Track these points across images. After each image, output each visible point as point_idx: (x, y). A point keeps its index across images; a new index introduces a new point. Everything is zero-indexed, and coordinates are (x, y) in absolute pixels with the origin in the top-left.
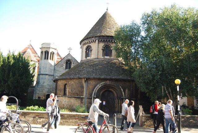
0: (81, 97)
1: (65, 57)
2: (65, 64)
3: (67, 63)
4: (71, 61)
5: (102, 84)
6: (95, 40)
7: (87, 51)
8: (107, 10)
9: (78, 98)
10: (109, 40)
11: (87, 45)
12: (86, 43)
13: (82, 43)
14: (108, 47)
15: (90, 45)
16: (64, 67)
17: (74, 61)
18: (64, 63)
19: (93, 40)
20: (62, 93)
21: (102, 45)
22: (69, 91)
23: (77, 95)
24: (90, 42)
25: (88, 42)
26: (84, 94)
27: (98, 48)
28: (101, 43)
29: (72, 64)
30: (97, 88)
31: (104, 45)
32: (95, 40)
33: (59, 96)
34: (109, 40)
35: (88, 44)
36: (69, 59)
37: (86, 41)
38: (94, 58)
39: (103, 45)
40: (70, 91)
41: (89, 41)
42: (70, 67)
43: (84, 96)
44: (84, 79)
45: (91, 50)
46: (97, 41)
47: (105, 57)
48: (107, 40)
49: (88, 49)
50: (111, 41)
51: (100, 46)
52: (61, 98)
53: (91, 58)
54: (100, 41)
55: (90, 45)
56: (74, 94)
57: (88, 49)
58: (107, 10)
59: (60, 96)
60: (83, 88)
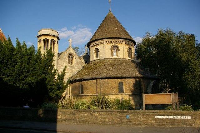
2: (68, 58)
6: (122, 41)
9: (136, 94)
13: (105, 41)
15: (117, 44)
16: (67, 61)
21: (126, 47)
22: (126, 89)
23: (136, 92)
24: (118, 42)
25: (115, 42)
26: (143, 91)
29: (74, 58)
32: (123, 42)
35: (114, 44)
37: (113, 40)
39: (128, 47)
42: (72, 64)
46: (124, 43)
53: (119, 58)
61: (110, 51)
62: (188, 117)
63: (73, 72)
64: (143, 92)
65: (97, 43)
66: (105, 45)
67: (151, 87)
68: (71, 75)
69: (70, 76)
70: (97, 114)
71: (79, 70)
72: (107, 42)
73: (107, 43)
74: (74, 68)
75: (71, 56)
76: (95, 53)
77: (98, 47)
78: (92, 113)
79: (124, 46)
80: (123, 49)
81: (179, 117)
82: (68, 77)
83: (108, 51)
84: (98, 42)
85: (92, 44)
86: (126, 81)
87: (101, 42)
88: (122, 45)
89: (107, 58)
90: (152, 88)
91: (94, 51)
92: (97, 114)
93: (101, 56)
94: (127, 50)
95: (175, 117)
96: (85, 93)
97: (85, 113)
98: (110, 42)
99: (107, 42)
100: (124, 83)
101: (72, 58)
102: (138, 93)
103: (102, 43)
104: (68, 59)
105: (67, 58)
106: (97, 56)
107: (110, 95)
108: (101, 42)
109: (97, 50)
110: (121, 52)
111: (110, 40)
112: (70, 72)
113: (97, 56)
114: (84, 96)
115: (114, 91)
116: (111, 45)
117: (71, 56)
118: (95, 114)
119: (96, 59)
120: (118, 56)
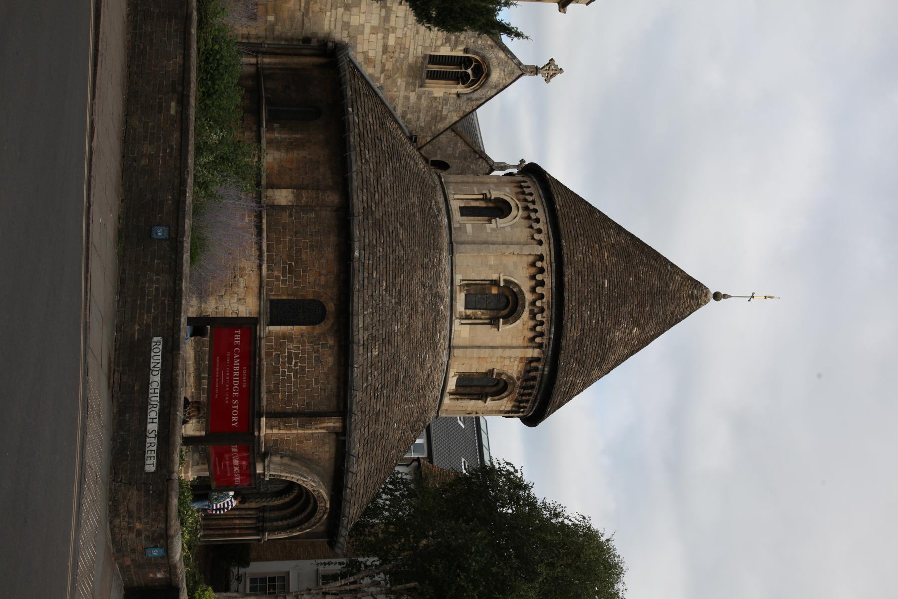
0: (263, 420)
1: (502, 55)
2: (459, 53)
3: (464, 62)
4: (474, 82)
5: (320, 492)
7: (494, 291)
8: (717, 296)
10: (530, 394)
11: (525, 285)
12: (539, 290)
13: (543, 250)
14: (502, 385)
15: (526, 314)
17: (476, 95)
18: (466, 50)
19: (541, 334)
20: (283, 290)
22: (289, 338)
23: (269, 391)
24: (539, 317)
25: (538, 303)
26: (275, 431)
27: (501, 357)
28: (521, 365)
29: (461, 89)
30: (304, 481)
31: (511, 378)
32: (540, 346)
33: (260, 267)
34: (530, 394)
35: (529, 297)
36: (488, 75)
38: (455, 342)
39: (510, 372)
40: (291, 346)
41: (542, 310)
42: (434, 76)
43: (269, 432)
44: (344, 427)
45: (494, 322)
46: (535, 353)
47: (455, 379)
48: (532, 387)
49: (507, 293)
50: (524, 398)
51: (507, 362)
52: (255, 284)
53: (456, 322)
54: (533, 364)
55: (526, 314)
56: (275, 371)
57: (507, 293)
58: (717, 296)
59: (264, 267)
60: (302, 426)
61: (495, 277)
62: (153, 461)
63: (389, 82)
64: (272, 428)
65: (535, 211)
66: (526, 250)
67: (294, 478)
68: (368, 71)
69: (369, 61)
70: (173, 112)
71: (398, 113)
72: (539, 264)
73: (533, 265)
74: (407, 84)
75: (469, 71)
76: (485, 199)
77: (517, 214)
78: (180, 89)
79: (519, 353)
80: (504, 347)
81: (152, 427)
82: (359, 48)
83: (491, 267)
84: (541, 215)
85: (533, 188)
86: (331, 342)
87: (539, 231)
88: (520, 342)
89: (459, 258)
90: (291, 485)
91: (495, 194)
92: (173, 112)
93: (469, 226)
94: (498, 368)
95: (153, 414)
96: (270, 129)
97: (179, 59)
98: (539, 277)
99: (539, 264)
100: (318, 329)
101: (462, 79)
102: (264, 403)
103: (537, 236)
104: (454, 54)
105: (461, 48)
106: (466, 211)
107: (260, 257)
108: (539, 231)
109: (500, 209)
110: (486, 334)
111: (547, 278)
112: (389, 66)
113: (466, 211)
114: (259, 125)
115: (277, 278)
116: (525, 285)
117: (469, 71)
118: (173, 104)
119: (455, 205)
120: (461, 318)
